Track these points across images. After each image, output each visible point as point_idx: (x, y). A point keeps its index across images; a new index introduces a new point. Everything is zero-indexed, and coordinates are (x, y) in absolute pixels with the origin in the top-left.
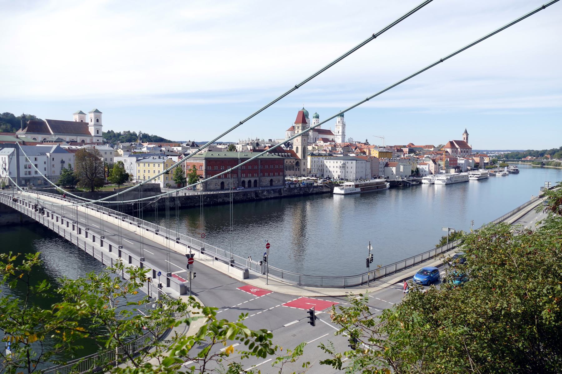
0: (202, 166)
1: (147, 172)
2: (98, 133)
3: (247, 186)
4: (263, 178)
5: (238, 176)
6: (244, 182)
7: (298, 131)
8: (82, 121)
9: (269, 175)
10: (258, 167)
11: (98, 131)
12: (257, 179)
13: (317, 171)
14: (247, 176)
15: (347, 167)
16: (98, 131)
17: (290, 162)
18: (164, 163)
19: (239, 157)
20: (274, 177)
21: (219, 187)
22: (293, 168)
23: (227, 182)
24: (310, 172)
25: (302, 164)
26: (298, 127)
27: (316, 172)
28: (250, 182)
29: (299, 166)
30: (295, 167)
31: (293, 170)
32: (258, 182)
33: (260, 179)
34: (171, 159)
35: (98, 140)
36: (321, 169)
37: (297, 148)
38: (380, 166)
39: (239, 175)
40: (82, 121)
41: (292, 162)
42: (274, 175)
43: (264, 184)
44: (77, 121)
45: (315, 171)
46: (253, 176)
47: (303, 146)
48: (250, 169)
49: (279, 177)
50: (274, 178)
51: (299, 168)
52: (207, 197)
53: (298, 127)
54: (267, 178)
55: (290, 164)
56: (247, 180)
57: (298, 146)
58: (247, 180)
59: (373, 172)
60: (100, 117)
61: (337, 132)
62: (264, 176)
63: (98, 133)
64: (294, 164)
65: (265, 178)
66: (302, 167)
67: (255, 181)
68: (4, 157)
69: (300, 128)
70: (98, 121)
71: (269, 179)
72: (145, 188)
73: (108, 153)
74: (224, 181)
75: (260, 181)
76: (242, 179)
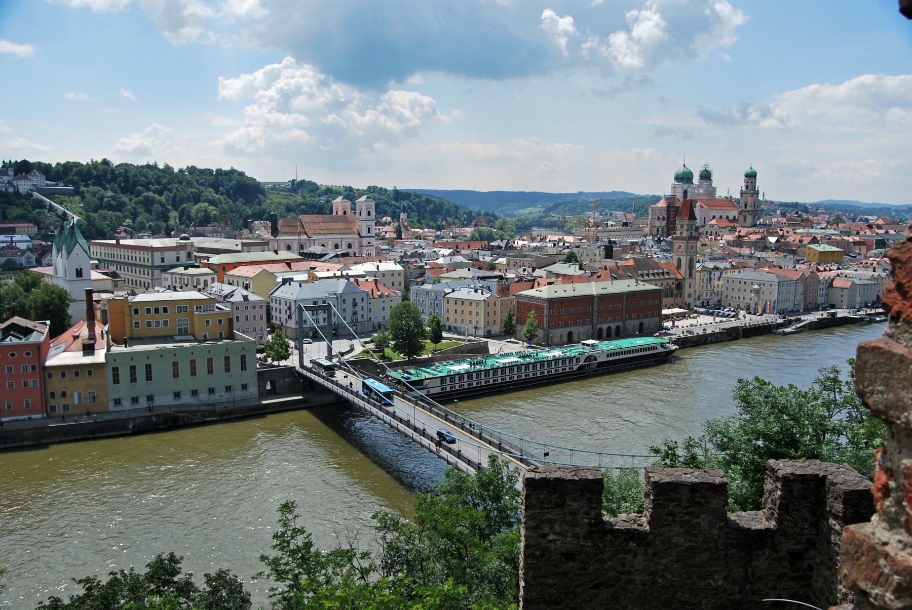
2: (369, 232)
3: (605, 335)
4: (629, 322)
6: (601, 329)
7: (681, 233)
9: (638, 318)
11: (369, 229)
12: (621, 324)
13: (711, 295)
14: (605, 322)
15: (763, 292)
16: (369, 229)
17: (668, 284)
19: (594, 293)
21: (565, 339)
22: (672, 293)
24: (699, 297)
25: (687, 285)
26: (682, 226)
27: (709, 297)
28: (609, 329)
29: (681, 289)
30: (675, 292)
31: (672, 297)
32: (621, 328)
33: (624, 324)
35: (369, 243)
36: (718, 292)
37: (680, 260)
38: (820, 287)
39: (595, 319)
41: (670, 283)
42: (646, 316)
45: (707, 295)
46: (614, 321)
47: (689, 258)
50: (646, 321)
51: (681, 294)
53: (682, 226)
55: (668, 287)
56: (605, 327)
57: (681, 257)
58: (605, 327)
59: (808, 299)
61: (744, 206)
62: (630, 318)
63: (369, 232)
64: (673, 286)
66: (687, 290)
67: (618, 328)
69: (685, 227)
73: (396, 275)
75: (625, 326)
76: (599, 326)
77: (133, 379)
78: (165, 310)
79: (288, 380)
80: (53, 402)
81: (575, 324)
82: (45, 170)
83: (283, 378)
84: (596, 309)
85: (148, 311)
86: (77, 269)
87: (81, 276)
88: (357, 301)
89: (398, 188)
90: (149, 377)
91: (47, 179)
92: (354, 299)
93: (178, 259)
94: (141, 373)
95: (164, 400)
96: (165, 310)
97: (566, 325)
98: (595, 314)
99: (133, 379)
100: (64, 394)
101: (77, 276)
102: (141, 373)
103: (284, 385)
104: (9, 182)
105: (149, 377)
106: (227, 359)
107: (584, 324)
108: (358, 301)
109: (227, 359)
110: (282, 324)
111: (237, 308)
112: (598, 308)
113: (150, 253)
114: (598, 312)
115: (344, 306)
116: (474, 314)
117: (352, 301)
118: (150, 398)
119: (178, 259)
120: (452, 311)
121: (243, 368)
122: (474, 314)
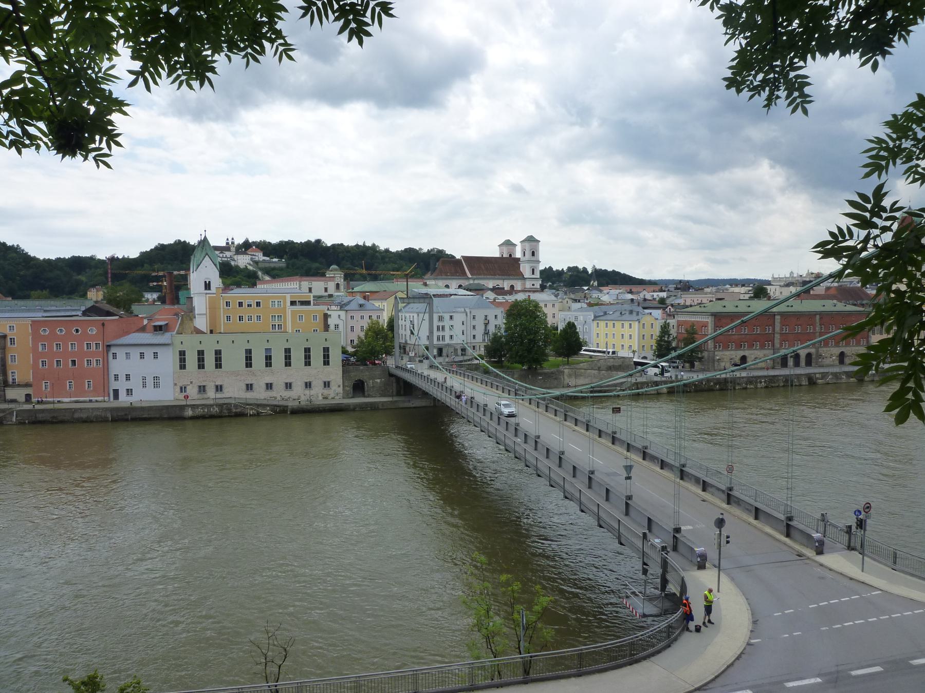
0: (706, 327)
1: (610, 336)
2: (533, 273)
4: (825, 349)
5: (773, 345)
8: (510, 255)
10: (814, 329)
11: (533, 270)
18: (639, 322)
20: (848, 348)
23: (753, 357)
32: (814, 356)
33: (817, 351)
34: (651, 314)
35: (533, 285)
39: (777, 342)
40: (510, 255)
43: (827, 361)
44: (504, 256)
48: (797, 333)
49: (857, 348)
52: (715, 384)
54: (832, 349)
60: (537, 248)
63: (533, 273)
65: (828, 349)
67: (809, 356)
68: (412, 315)
70: (533, 254)
71: (836, 351)
72: (609, 364)
74: (746, 355)
77: (201, 366)
78: (258, 304)
79: (378, 381)
80: (114, 385)
81: (751, 346)
82: (265, 248)
83: (373, 378)
84: (777, 329)
85: (241, 304)
86: (205, 282)
87: (209, 289)
88: (488, 318)
89: (598, 267)
90: (218, 365)
91: (264, 256)
92: (486, 316)
93: (326, 290)
94: (210, 360)
95: (234, 392)
96: (258, 304)
97: (739, 347)
98: (777, 336)
99: (201, 366)
100: (128, 377)
101: (206, 289)
102: (210, 360)
103: (373, 387)
104: (231, 257)
105: (218, 365)
106: (307, 350)
107: (762, 347)
108: (491, 318)
109: (307, 350)
110: (406, 341)
111: (352, 317)
112: (782, 329)
113: (298, 282)
114: (781, 334)
115: (474, 323)
116: (627, 336)
117: (483, 318)
118: (219, 388)
119: (326, 290)
120: (602, 336)
121: (326, 363)
122: (627, 336)
